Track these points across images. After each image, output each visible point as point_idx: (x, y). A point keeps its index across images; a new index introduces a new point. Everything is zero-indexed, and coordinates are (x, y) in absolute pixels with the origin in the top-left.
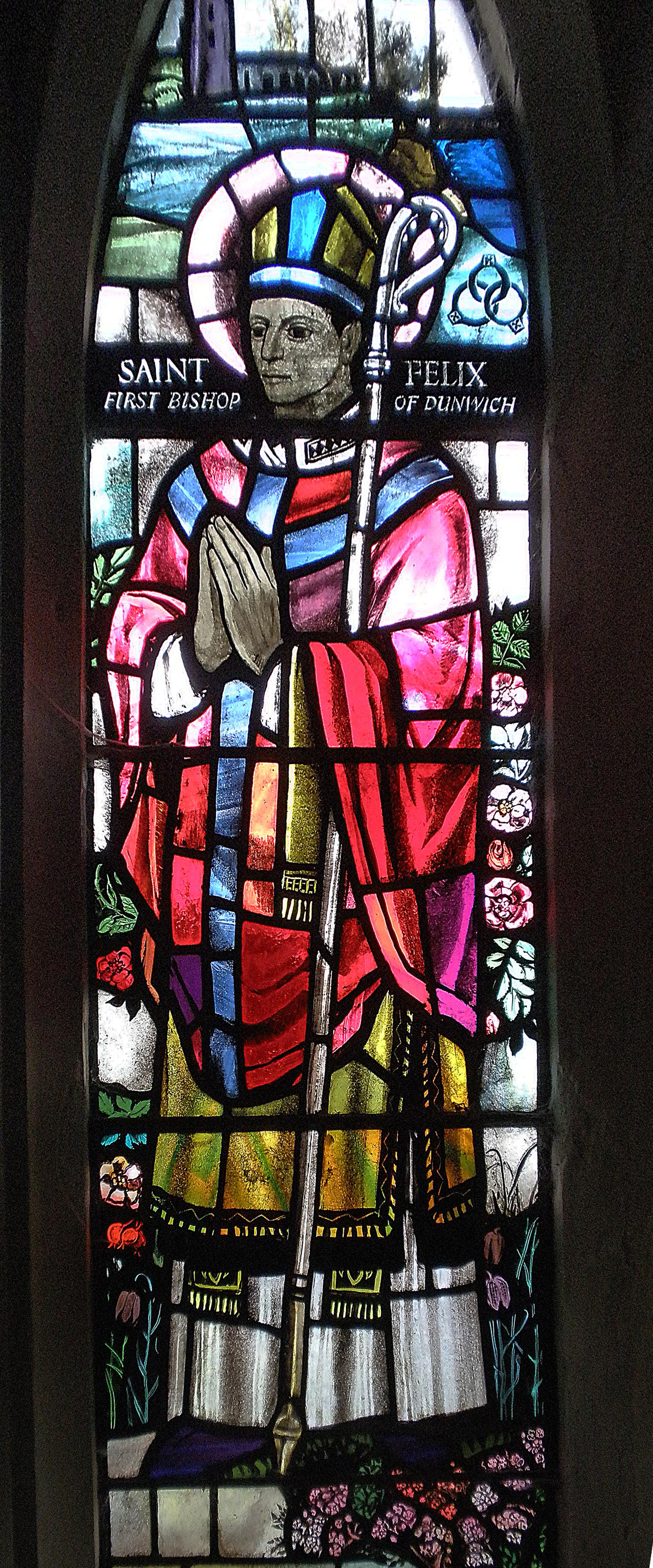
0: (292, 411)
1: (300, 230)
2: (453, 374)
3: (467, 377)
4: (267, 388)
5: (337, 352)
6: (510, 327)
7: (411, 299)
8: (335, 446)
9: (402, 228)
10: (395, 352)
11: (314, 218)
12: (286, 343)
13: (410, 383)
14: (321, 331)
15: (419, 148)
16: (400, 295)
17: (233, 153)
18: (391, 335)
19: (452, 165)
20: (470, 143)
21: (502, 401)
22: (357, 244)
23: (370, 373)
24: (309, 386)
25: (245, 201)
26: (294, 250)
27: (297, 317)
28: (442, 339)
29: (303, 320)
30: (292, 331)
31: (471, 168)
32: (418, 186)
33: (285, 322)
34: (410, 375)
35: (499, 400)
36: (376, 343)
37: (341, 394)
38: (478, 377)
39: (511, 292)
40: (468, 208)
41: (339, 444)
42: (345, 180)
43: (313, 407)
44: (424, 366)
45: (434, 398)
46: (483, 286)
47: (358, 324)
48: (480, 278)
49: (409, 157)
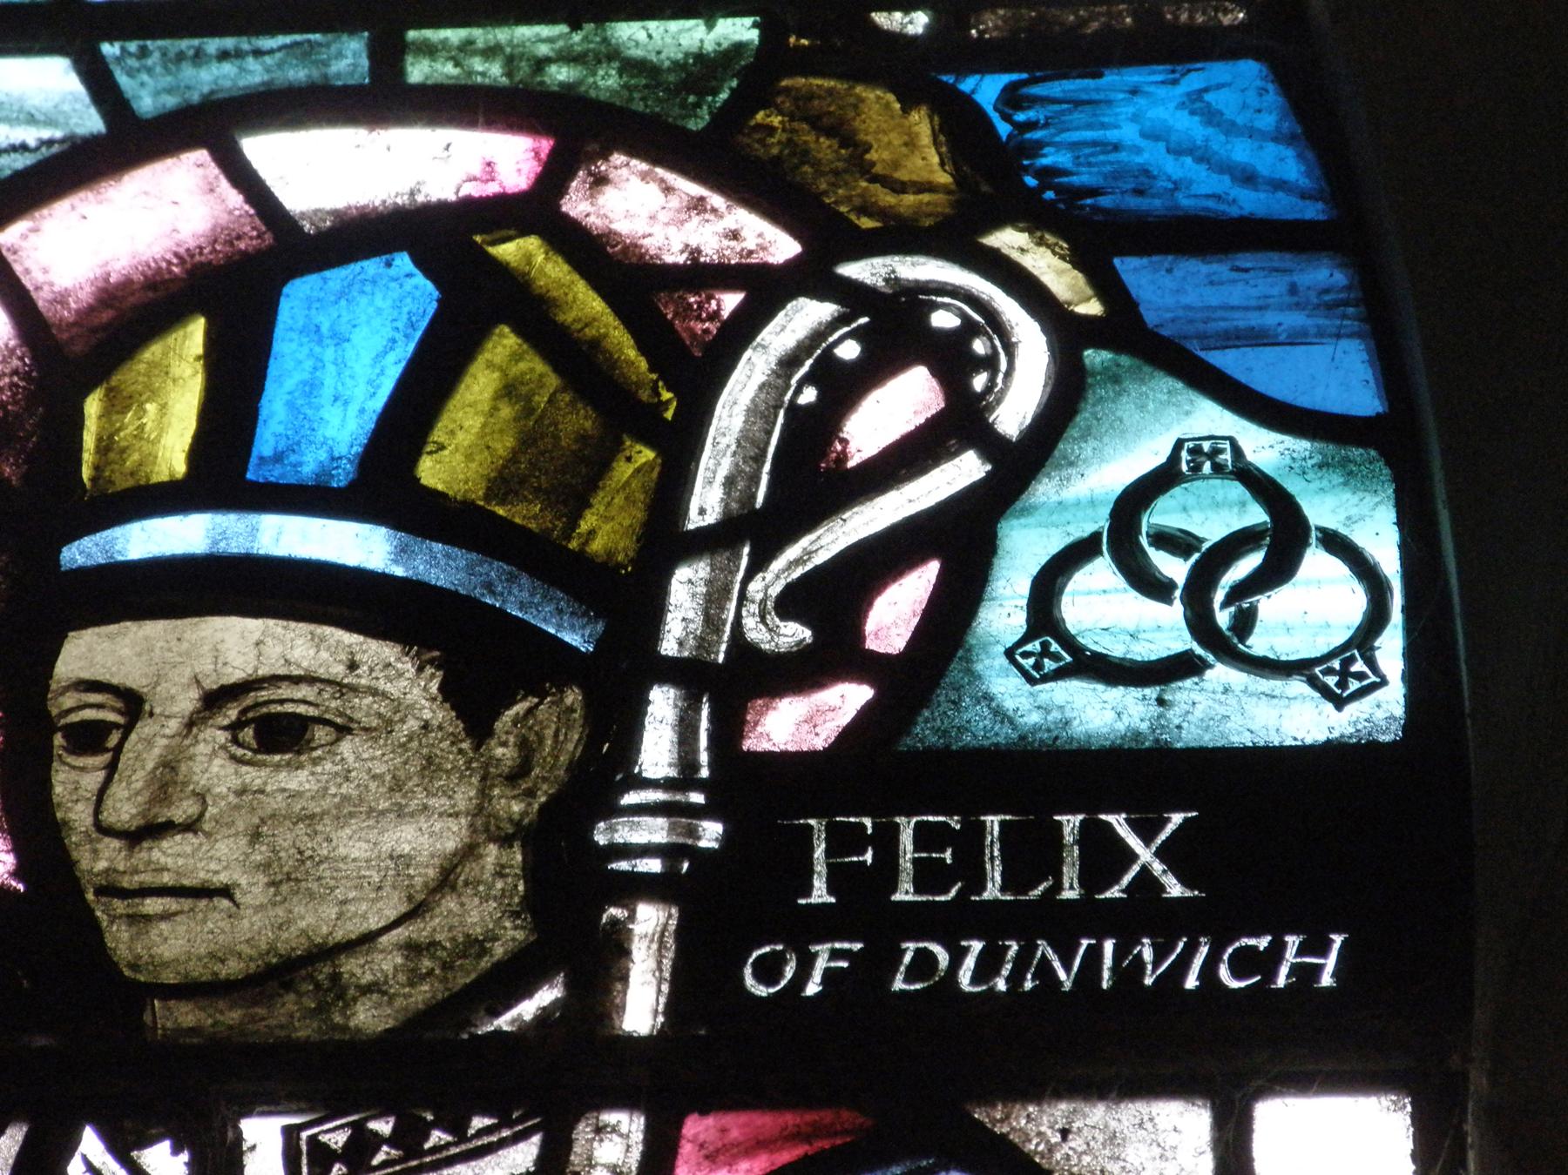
0: (234, 1016)
1: (311, 387)
2: (1032, 854)
3: (1104, 856)
4: (119, 939)
5: (465, 796)
6: (1313, 682)
7: (834, 598)
8: (437, 1137)
9: (789, 363)
10: (746, 785)
11: (379, 343)
12: (215, 768)
13: (820, 894)
14: (388, 725)
15: (875, 105)
16: (775, 591)
17: (23, 148)
18: (729, 729)
19: (1036, 148)
20: (1111, 78)
21: (1277, 949)
22: (579, 421)
23: (624, 865)
24: (316, 920)
25: (61, 299)
26: (278, 458)
27: (275, 680)
28: (978, 727)
29: (304, 691)
30: (248, 734)
31: (1123, 156)
32: (866, 223)
33: (214, 700)
34: (820, 867)
35: (1263, 943)
36: (657, 752)
37: (475, 946)
38: (1157, 867)
39: (1317, 562)
40: (1105, 283)
41: (458, 1129)
42: (535, 210)
43: (339, 992)
44: (886, 840)
45: (937, 949)
46: (1177, 543)
47: (573, 697)
48: (1165, 513)
49: (830, 132)
